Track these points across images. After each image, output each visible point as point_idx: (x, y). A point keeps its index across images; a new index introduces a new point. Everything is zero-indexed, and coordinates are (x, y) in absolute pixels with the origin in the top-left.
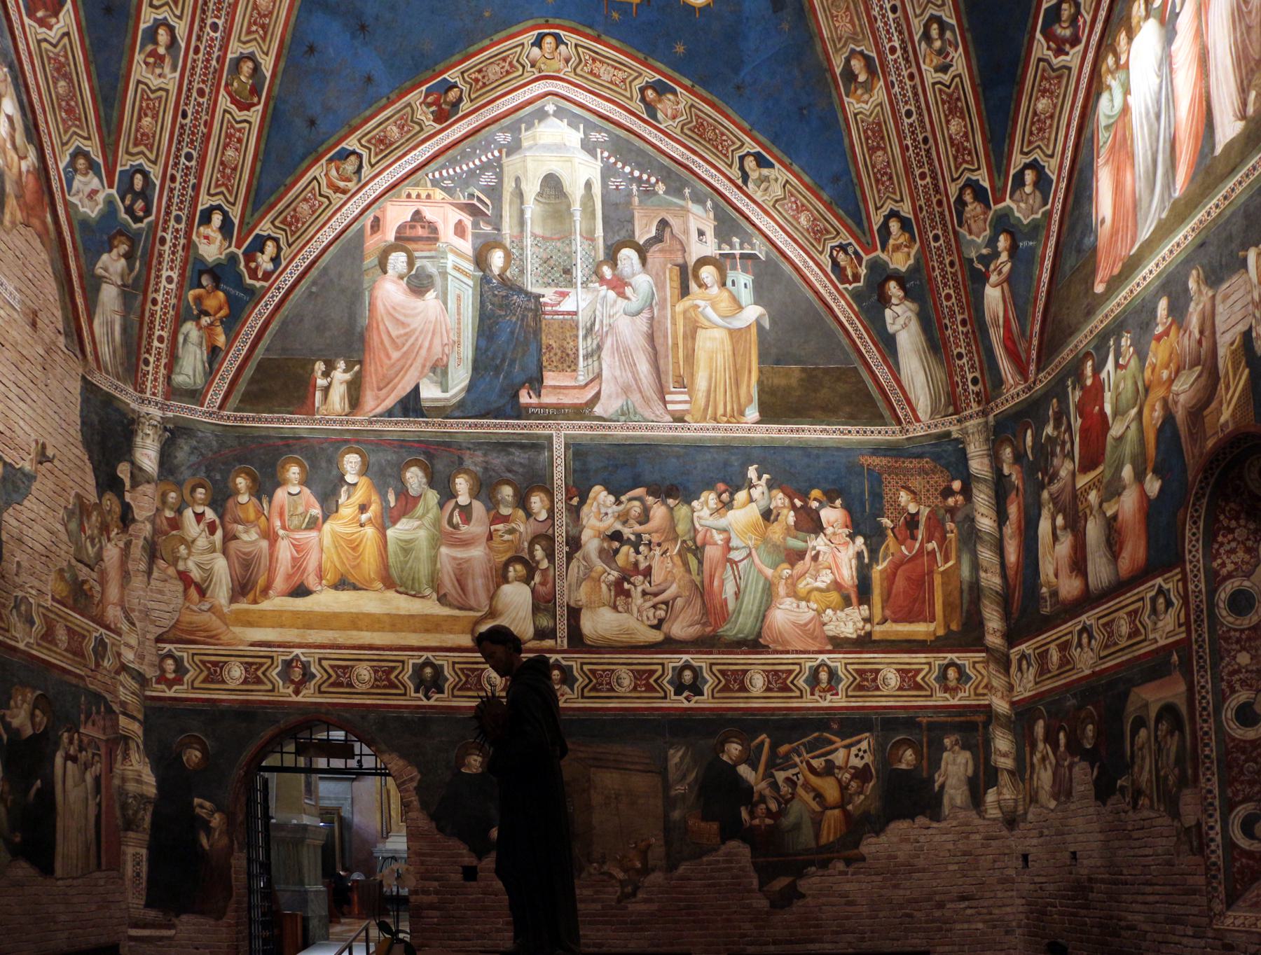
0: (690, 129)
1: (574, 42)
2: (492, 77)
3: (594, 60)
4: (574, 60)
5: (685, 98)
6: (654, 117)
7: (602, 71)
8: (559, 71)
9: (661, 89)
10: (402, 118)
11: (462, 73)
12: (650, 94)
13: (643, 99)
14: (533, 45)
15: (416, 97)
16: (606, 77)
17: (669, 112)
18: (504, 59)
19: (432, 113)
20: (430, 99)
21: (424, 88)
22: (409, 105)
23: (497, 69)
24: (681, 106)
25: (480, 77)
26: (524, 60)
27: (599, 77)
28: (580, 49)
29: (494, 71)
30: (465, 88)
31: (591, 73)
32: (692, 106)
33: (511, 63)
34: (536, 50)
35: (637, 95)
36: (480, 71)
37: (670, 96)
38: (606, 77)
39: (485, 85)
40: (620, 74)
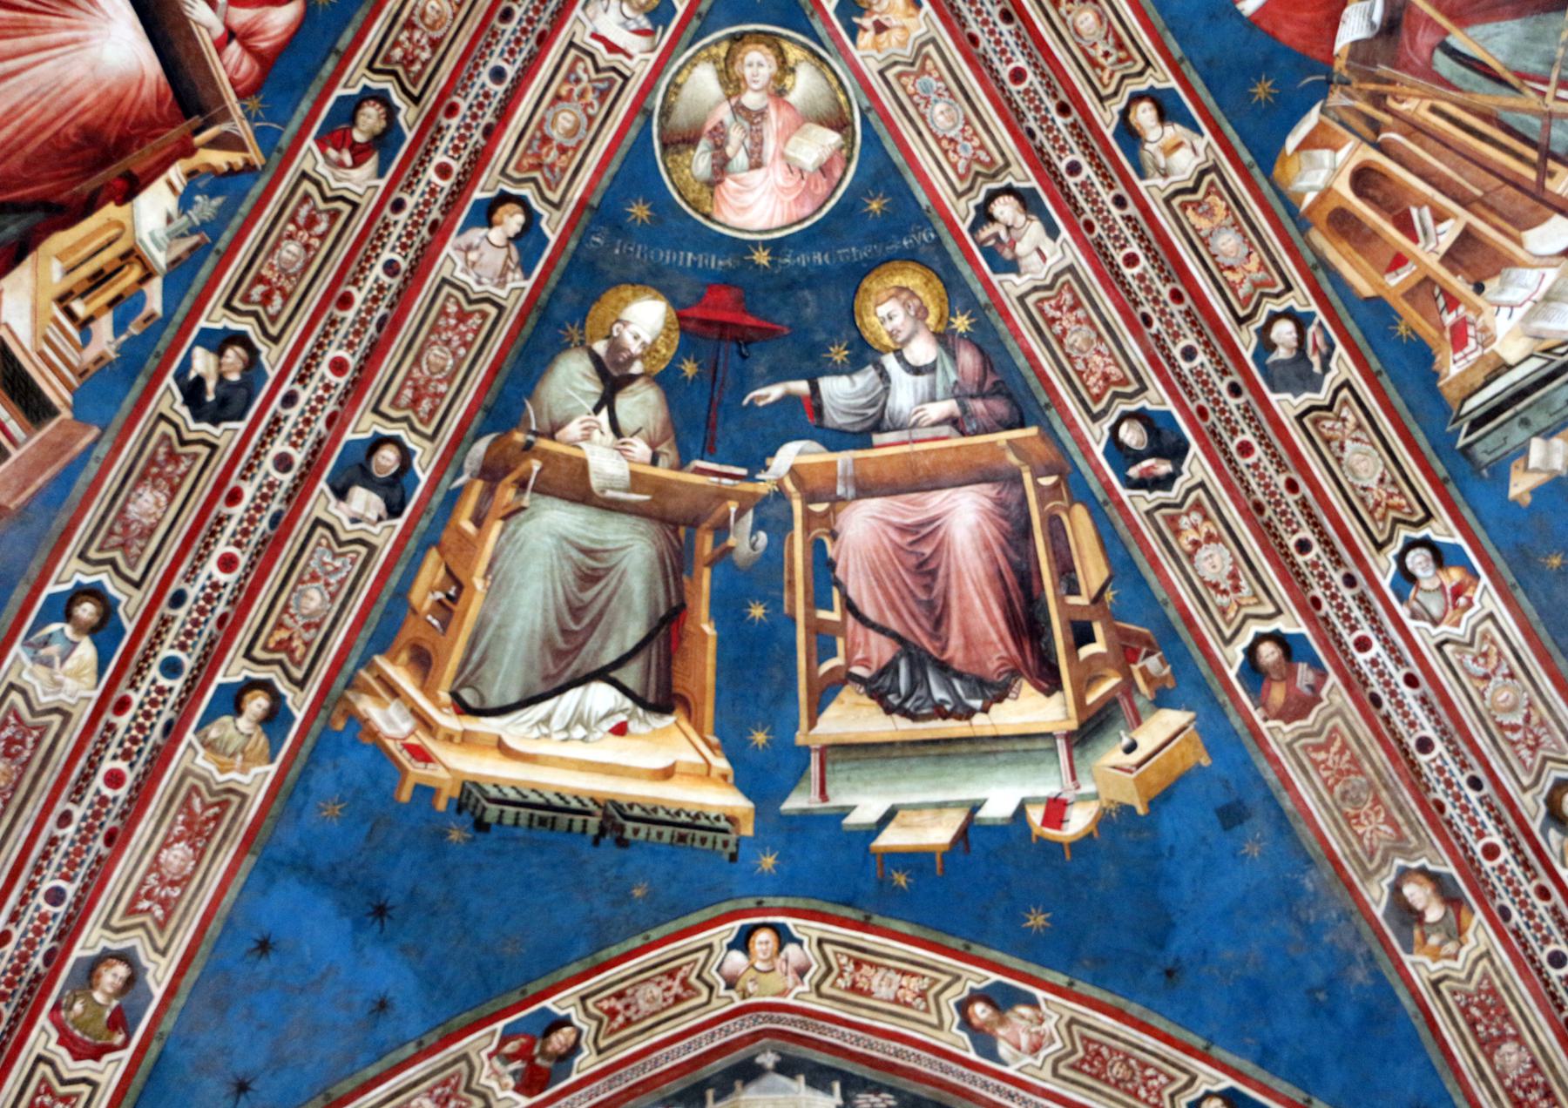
0: (1073, 1067)
1: (815, 935)
2: (644, 1007)
3: (858, 964)
4: (816, 969)
5: (1055, 1010)
6: (992, 1054)
7: (875, 981)
8: (784, 993)
9: (1000, 999)
10: (445, 1083)
11: (583, 999)
12: (980, 1011)
13: (966, 1023)
14: (731, 947)
15: (479, 1044)
16: (884, 991)
17: (1024, 1041)
18: (671, 974)
19: (514, 1073)
20: (511, 1047)
21: (500, 1026)
22: (465, 1057)
23: (657, 991)
24: (1048, 1026)
25: (619, 1006)
26: (712, 974)
27: (869, 994)
28: (828, 948)
29: (649, 995)
30: (588, 1027)
31: (854, 988)
32: (1072, 1021)
33: (685, 983)
34: (737, 957)
35: (951, 1017)
36: (620, 995)
37: (1024, 1010)
38: (884, 991)
39: (628, 1022)
40: (915, 984)
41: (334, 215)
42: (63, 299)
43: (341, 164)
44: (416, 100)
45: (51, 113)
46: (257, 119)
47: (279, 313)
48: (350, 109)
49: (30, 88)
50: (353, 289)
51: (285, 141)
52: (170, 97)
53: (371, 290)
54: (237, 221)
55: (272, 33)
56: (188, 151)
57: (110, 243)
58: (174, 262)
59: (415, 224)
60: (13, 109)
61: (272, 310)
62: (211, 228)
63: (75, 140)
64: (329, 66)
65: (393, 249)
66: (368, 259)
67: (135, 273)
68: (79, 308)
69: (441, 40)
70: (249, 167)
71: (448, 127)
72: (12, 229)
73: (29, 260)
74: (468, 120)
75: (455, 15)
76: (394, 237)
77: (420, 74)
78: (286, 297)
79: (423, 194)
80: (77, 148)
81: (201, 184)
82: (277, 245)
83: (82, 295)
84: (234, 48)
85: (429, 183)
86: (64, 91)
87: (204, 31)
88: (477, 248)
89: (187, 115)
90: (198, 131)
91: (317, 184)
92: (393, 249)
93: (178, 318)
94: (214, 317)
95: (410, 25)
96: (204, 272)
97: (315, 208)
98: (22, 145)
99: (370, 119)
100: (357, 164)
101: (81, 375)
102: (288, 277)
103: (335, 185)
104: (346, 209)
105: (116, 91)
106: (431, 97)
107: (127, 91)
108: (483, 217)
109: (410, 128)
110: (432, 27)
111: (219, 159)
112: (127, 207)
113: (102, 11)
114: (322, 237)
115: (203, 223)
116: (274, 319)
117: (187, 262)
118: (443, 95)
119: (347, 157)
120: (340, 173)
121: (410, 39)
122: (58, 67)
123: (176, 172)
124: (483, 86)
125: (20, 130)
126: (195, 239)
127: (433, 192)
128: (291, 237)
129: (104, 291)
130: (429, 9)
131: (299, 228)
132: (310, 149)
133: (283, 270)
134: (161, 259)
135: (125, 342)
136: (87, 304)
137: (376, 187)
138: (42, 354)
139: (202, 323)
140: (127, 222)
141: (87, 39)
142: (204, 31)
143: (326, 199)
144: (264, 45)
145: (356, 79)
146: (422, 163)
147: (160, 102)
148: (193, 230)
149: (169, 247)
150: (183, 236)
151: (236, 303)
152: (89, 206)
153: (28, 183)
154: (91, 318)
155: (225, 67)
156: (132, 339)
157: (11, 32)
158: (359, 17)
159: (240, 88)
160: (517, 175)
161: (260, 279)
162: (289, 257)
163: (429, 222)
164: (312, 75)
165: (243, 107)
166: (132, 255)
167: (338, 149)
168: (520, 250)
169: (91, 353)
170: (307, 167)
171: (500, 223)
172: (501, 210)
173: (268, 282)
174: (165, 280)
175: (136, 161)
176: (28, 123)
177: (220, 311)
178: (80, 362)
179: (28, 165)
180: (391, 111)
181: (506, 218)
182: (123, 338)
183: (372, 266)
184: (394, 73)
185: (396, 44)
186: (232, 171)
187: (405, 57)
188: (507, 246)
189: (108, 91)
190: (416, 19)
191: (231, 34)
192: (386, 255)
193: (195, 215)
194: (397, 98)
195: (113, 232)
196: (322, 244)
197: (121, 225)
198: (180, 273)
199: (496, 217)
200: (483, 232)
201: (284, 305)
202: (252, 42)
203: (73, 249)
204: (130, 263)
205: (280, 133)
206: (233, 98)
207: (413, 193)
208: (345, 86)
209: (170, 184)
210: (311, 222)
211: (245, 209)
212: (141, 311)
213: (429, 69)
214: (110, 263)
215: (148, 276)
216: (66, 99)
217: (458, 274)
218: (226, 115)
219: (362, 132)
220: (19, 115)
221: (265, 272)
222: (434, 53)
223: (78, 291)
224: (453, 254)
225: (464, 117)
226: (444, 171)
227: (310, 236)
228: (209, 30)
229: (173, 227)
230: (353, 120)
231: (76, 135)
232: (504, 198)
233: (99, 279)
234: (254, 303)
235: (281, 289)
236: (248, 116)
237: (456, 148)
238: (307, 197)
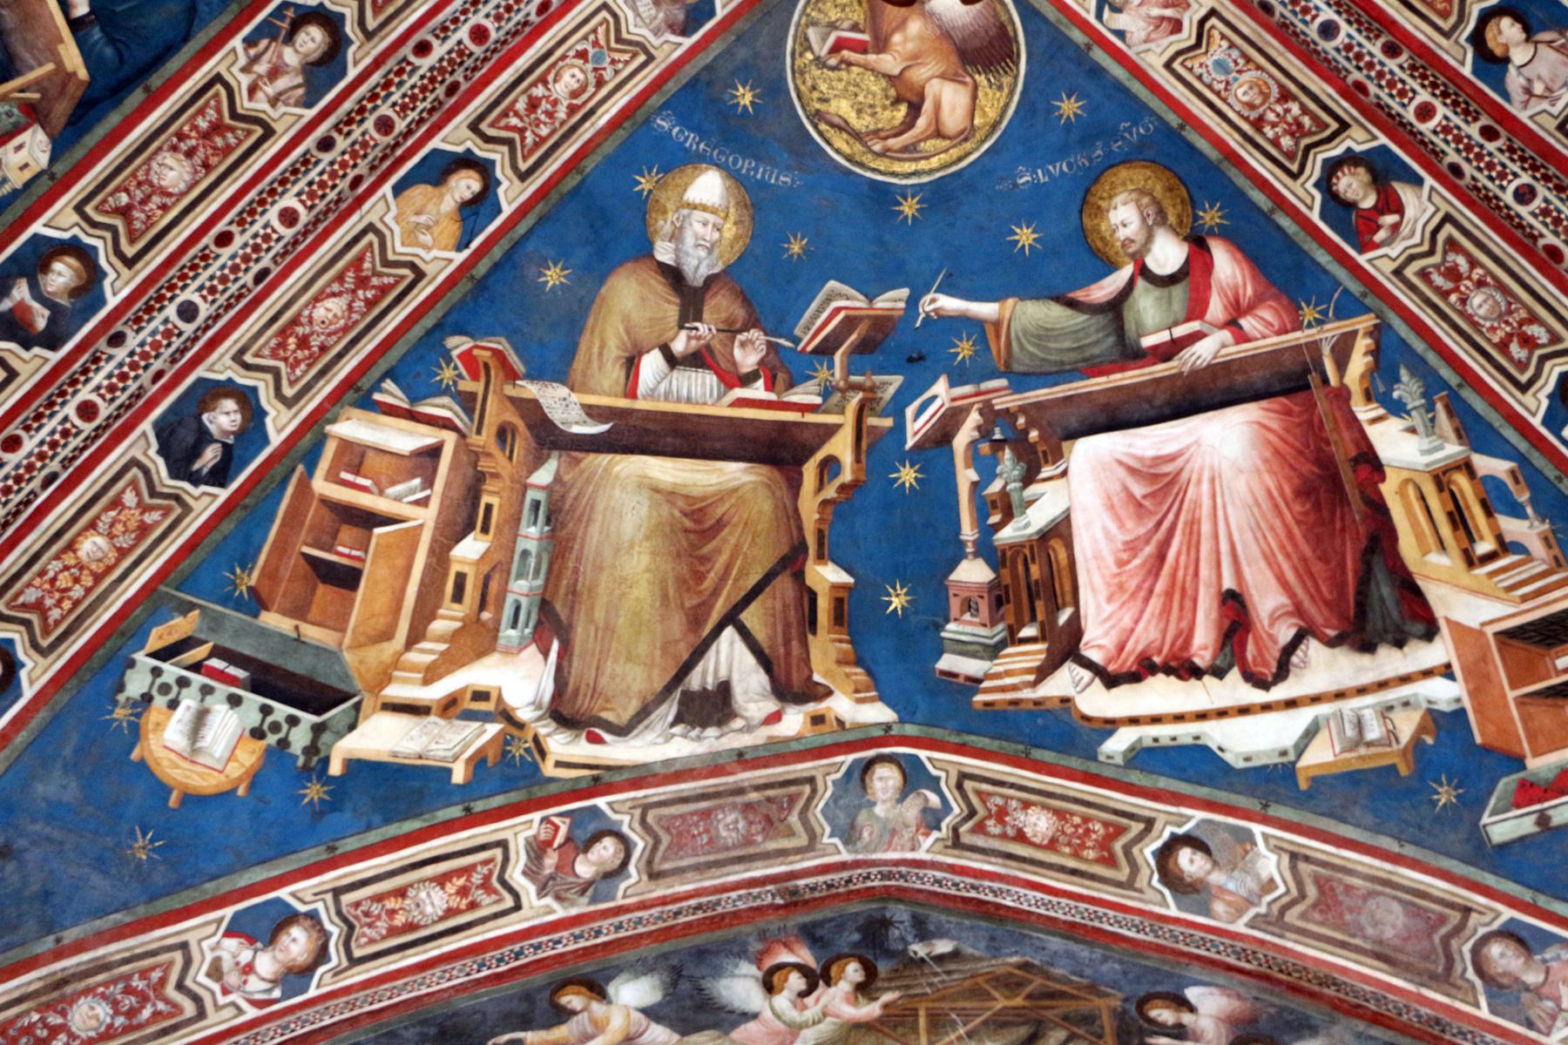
41: (1452, 244)
42: (1471, 561)
43: (1395, 228)
44: (1344, 126)
45: (1278, 524)
46: (1325, 313)
47: (1550, 330)
48: (1337, 206)
49: (1249, 536)
50: (1541, 242)
51: (1355, 287)
52: (1283, 400)
53: (1546, 225)
54: (1432, 358)
55: (1240, 280)
56: (1343, 395)
57: (1422, 498)
58: (1459, 436)
59: (1479, 157)
60: (1266, 558)
61: (1544, 338)
62: (1432, 386)
63: (1308, 506)
64: (1285, 222)
65: (1502, 188)
66: (1509, 217)
67: (1461, 481)
68: (1484, 547)
69: (1281, 86)
70: (1377, 332)
71: (1378, 97)
72: (1385, 590)
73: (1420, 583)
74: (1373, 74)
75: (1259, 67)
76: (1489, 184)
77: (1314, 118)
78: (1533, 319)
79: (1447, 142)
80: (1317, 506)
81: (1382, 389)
82: (1469, 318)
83: (1472, 540)
84: (1247, 323)
85: (1435, 132)
86: (1257, 503)
87: (1224, 351)
88: (1529, 80)
89: (1307, 387)
90: (1325, 381)
91: (1412, 258)
92: (1502, 188)
93: (1523, 446)
94: (1533, 408)
95: (1258, 124)
96: (1479, 405)
97: (1437, 267)
98: (1304, 559)
99: (1352, 184)
100: (1399, 209)
101: (1559, 565)
102: (1510, 312)
103: (1417, 239)
104: (1448, 229)
105: (1268, 454)
106: (1344, 108)
107: (1269, 442)
108: (1495, 68)
109: (1375, 138)
110: (1266, 96)
111: (1359, 362)
112: (1387, 470)
113: (1188, 447)
114: (1473, 263)
115: (1424, 395)
116: (1555, 338)
117: (1462, 423)
118: (1345, 94)
119: (1390, 219)
120: (1405, 230)
121: (1274, 125)
122: (1233, 503)
123: (1364, 412)
124: (1337, 50)
125: (1288, 556)
126: (1439, 407)
127: (1446, 130)
128: (1464, 301)
129: (1473, 518)
130: (1245, 99)
131: (1457, 289)
132: (1370, 261)
133: (1500, 316)
134: (1453, 449)
135: (1535, 510)
136: (1482, 538)
137: (1432, 188)
138: (1524, 598)
139: (1536, 422)
140: (1405, 475)
141: (1212, 468)
142: (1224, 351)
143: (1431, 252)
144: (1249, 291)
145: (1305, 195)
146: (1412, 133)
147: (1288, 412)
148: (1430, 408)
149: (1441, 437)
150: (1433, 420)
151: (1524, 378)
152: (1379, 509)
153: (1342, 565)
154: (1499, 538)
155: (1264, 337)
156: (1534, 501)
157: (1194, 538)
158: (1241, 181)
159: (1289, 327)
160: (1453, 19)
161: (1503, 346)
162: (1486, 307)
163: (1481, 140)
164: (1290, 244)
165: (1310, 326)
166: (1441, 479)
167: (1379, 227)
168: (1545, 28)
169: (1537, 548)
170: (1389, 267)
171: (1507, 47)
172: (1491, 44)
173: (1510, 336)
174: (1477, 450)
175: (1342, 450)
176: (1282, 547)
177: (1528, 398)
178: (1544, 561)
179: (1324, 559)
180: (1350, 159)
181: (1502, 40)
182: (1529, 510)
183: (1518, 216)
184: (1308, 148)
185: (1275, 143)
186: (1376, 352)
187: (1292, 134)
188: (1536, 43)
189: (1266, 461)
190: (1253, 115)
191: (1232, 324)
192: (1508, 197)
193: (1414, 401)
194: (1336, 150)
195: (1411, 491)
196: (1482, 266)
197: (1407, 481)
198: (1474, 433)
199: (1498, 52)
200: (1512, 70)
201: (1542, 323)
202: (1244, 303)
203: (1419, 536)
204: (1449, 482)
205: (1346, 291)
206: (1298, 334)
207: (1443, 152)
208: (1310, 208)
209: (1374, 421)
210: (1453, 274)
211: (1419, 346)
212: (1505, 485)
213: (1312, 106)
214: (1444, 505)
215: (1467, 467)
216: (1266, 505)
217: (1555, 110)
218: (1315, 346)
219: (1365, 197)
220: (1273, 554)
221: (1496, 339)
222: (1295, 98)
223: (1466, 544)
224: (1530, 112)
225: (1369, 77)
226: (1425, 112)
227: (1469, 278)
228: (1224, 346)
229: (1420, 429)
230: (1351, 206)
231: (1303, 505)
232: (1477, 39)
233: (1458, 518)
234: (1529, 359)
235: (1521, 323)
236: (1320, 322)
237: (1402, 93)
238: (1424, 274)
